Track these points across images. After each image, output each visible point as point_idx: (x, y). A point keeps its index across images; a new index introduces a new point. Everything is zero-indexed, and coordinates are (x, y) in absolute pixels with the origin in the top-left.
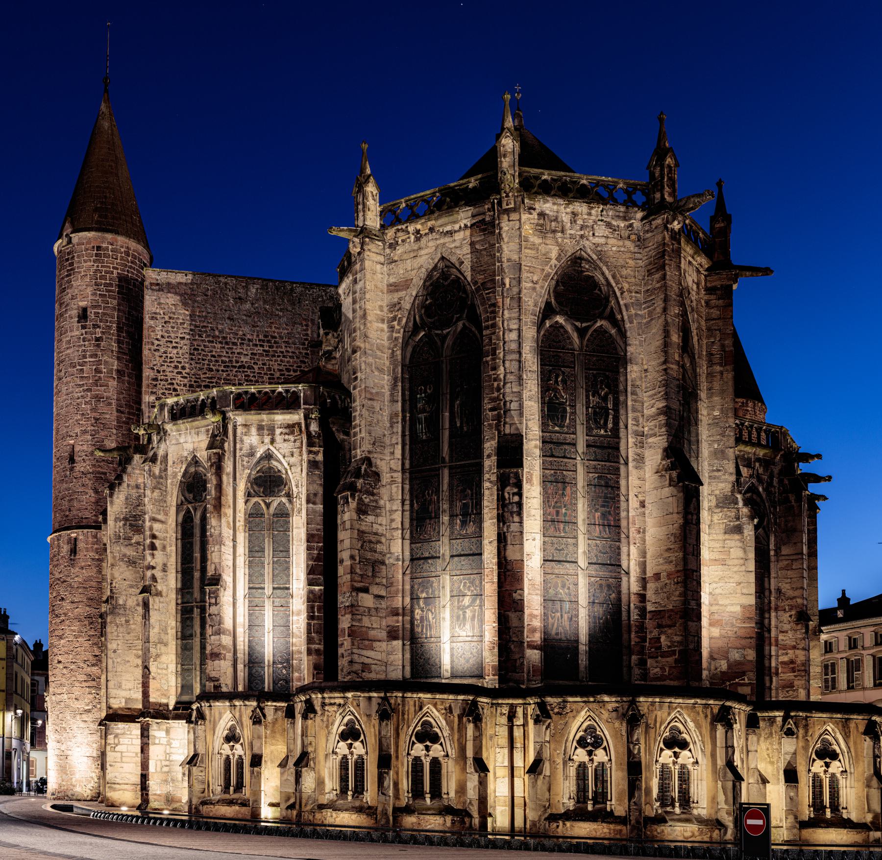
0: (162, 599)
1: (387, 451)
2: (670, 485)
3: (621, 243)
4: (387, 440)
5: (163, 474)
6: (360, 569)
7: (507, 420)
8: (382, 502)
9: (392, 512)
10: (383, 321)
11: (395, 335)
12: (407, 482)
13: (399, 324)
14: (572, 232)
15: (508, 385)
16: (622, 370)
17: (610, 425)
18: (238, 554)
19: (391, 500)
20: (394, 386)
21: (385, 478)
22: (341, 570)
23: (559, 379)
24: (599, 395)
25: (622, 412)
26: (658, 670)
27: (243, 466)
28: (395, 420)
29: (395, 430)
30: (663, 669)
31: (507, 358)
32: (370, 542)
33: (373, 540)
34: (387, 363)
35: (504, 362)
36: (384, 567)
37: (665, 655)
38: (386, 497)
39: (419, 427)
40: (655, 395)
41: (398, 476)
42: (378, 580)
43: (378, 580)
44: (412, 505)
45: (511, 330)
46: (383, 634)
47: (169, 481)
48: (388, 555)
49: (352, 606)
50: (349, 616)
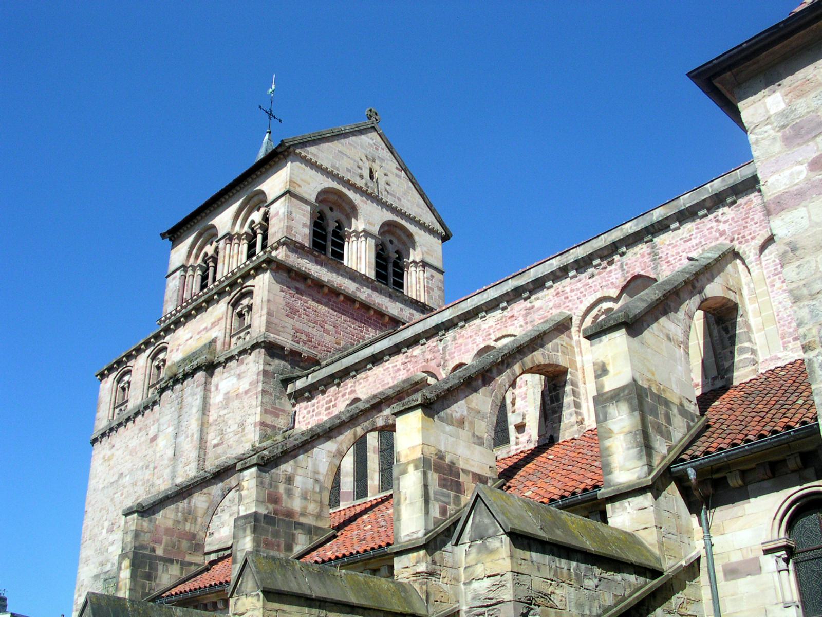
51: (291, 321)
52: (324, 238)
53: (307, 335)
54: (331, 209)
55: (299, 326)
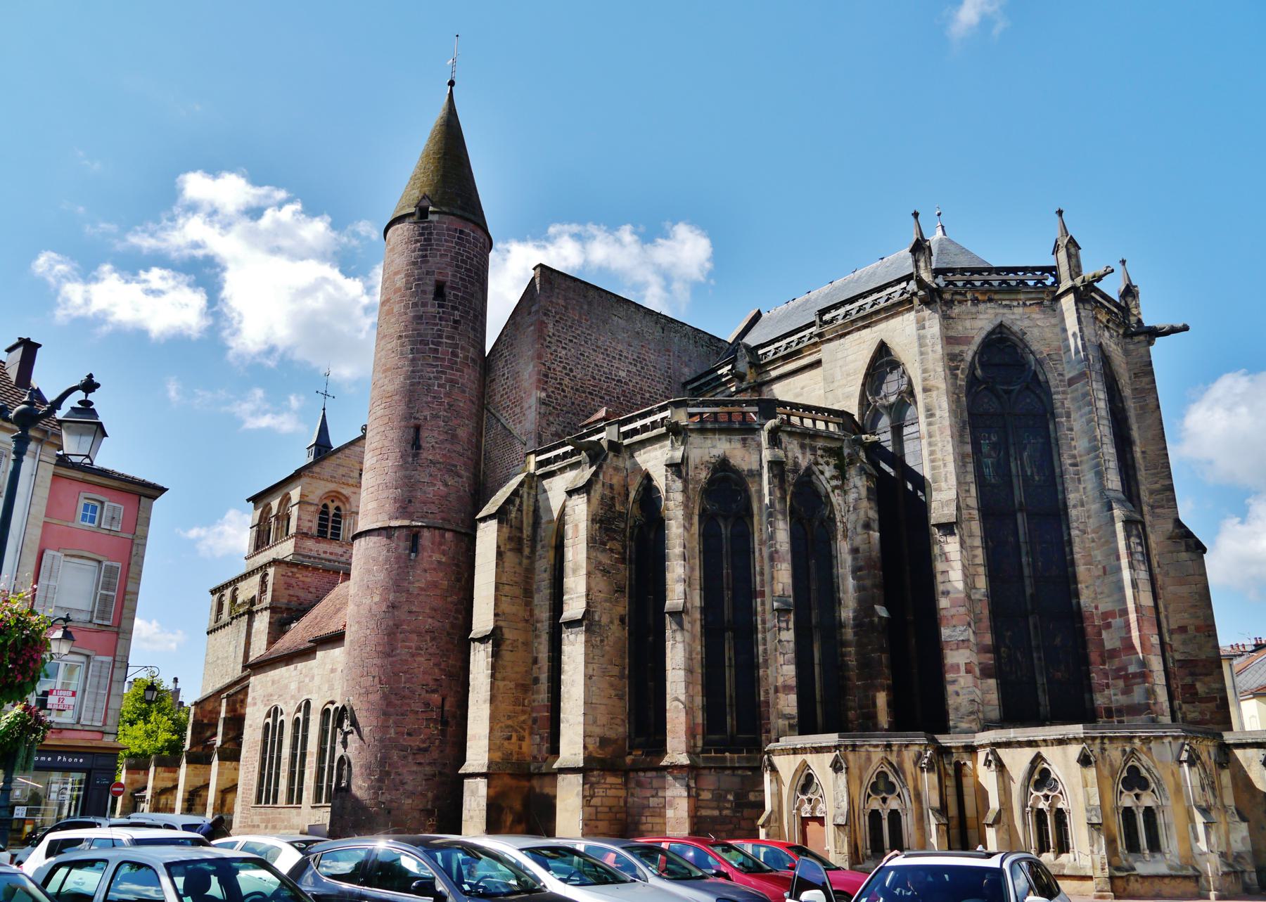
16: (1128, 449)
25: (1133, 483)
35: (1098, 424)
40: (1158, 473)
48: (974, 591)
51: (288, 592)
52: (327, 520)
53: (297, 596)
54: (333, 501)
55: (291, 592)
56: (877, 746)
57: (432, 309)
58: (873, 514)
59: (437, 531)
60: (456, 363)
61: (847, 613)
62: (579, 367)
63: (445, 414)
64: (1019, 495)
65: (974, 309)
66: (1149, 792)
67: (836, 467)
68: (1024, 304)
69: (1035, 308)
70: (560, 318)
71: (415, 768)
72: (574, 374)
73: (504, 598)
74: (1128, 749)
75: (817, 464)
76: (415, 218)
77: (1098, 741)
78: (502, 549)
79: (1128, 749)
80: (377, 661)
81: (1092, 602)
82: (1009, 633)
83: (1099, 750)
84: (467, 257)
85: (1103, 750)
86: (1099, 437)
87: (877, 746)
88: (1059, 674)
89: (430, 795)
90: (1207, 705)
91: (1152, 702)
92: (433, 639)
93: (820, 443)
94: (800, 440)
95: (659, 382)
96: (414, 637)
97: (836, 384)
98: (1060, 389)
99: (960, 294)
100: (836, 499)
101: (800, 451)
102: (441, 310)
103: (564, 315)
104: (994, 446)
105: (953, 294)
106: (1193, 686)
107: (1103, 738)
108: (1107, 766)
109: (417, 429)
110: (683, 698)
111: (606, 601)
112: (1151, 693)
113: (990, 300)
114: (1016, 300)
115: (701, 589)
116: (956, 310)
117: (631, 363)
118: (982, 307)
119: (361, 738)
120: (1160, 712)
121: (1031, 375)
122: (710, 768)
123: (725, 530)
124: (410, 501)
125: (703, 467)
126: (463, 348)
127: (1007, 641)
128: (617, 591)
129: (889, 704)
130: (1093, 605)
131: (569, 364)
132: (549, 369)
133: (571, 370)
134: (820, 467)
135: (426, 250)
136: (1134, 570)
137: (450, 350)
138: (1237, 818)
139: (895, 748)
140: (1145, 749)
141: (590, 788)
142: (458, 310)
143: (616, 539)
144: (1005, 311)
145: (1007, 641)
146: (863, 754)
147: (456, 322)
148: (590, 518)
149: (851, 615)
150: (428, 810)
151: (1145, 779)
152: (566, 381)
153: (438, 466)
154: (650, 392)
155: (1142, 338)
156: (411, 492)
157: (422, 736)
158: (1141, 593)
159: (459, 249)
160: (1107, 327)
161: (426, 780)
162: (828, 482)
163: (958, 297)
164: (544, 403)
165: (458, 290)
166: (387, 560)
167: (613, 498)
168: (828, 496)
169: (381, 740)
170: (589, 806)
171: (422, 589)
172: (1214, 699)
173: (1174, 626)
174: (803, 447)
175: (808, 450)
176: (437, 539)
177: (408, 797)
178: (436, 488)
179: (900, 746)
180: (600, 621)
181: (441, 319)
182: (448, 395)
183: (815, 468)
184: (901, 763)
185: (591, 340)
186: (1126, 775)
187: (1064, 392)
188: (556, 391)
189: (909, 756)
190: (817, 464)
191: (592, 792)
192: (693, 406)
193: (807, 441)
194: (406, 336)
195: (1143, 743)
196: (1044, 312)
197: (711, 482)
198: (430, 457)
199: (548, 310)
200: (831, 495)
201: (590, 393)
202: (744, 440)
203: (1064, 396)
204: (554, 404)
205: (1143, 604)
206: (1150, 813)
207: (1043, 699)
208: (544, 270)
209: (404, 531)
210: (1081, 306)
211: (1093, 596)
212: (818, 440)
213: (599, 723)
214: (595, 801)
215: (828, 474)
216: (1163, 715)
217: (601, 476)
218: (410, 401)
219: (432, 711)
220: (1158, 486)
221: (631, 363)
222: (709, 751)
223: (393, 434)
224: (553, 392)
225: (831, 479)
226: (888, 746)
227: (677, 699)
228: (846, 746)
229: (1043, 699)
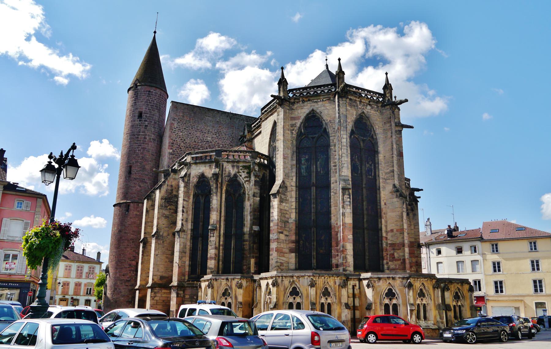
0: (185, 233)
1: (290, 178)
2: (396, 198)
3: (375, 112)
4: (290, 175)
5: (188, 182)
6: (281, 224)
7: (343, 170)
8: (288, 198)
9: (292, 202)
10: (289, 130)
11: (293, 136)
12: (298, 191)
13: (295, 132)
14: (360, 107)
15: (343, 158)
16: (376, 156)
17: (373, 175)
18: (222, 216)
19: (291, 197)
20: (293, 154)
21: (289, 189)
22: (271, 225)
23: (356, 157)
24: (369, 164)
25: (377, 170)
26: (394, 266)
27: (225, 180)
28: (293, 167)
29: (293, 171)
30: (396, 265)
31: (342, 148)
32: (284, 213)
33: (285, 213)
34: (290, 146)
36: (288, 224)
37: (396, 260)
38: (289, 196)
39: (302, 171)
40: (389, 165)
41: (294, 188)
42: (286, 229)
43: (286, 229)
44: (299, 199)
45: (344, 138)
46: (287, 251)
47: (191, 185)
48: (290, 219)
49: (277, 239)
50: (276, 243)
56: (223, 279)
57: (137, 122)
58: (257, 191)
59: (136, 204)
60: (146, 141)
61: (246, 229)
62: (188, 138)
63: (141, 161)
64: (314, 180)
65: (302, 105)
66: (298, 297)
67: (247, 173)
68: (323, 100)
69: (327, 102)
70: (180, 121)
71: (125, 287)
72: (186, 141)
73: (148, 227)
74: (291, 281)
75: (239, 172)
76: (133, 89)
77: (281, 277)
78: (148, 209)
79: (291, 281)
80: (115, 250)
81: (335, 222)
82: (304, 235)
83: (281, 281)
84: (152, 101)
85: (282, 281)
86: (341, 154)
87: (223, 279)
88: (322, 251)
89: (130, 296)
90: (398, 262)
91: (344, 262)
92: (133, 242)
93: (241, 164)
94: (232, 164)
95: (227, 140)
96: (126, 241)
97: (264, 138)
98: (333, 135)
99: (297, 99)
100: (246, 186)
101: (232, 168)
102: (140, 122)
103: (182, 119)
104: (307, 160)
105: (294, 100)
106: (393, 254)
107: (282, 276)
108: (283, 287)
109: (130, 167)
110: (178, 262)
111: (166, 227)
112: (345, 258)
113: (309, 100)
114: (319, 99)
115: (192, 222)
116: (296, 106)
117: (214, 134)
118: (306, 103)
119: (110, 277)
120: (347, 266)
121: (323, 130)
122: (189, 287)
123: (202, 201)
124: (127, 193)
125: (195, 177)
126: (149, 135)
127: (303, 238)
128: (171, 224)
129: (256, 263)
130: (336, 223)
131: (183, 138)
132: (174, 141)
133: (184, 140)
134: (240, 174)
135: (136, 100)
136: (344, 209)
137: (143, 137)
138: (345, 308)
139: (230, 280)
140: (297, 280)
141: (154, 294)
142: (147, 121)
143: (173, 205)
144: (315, 104)
145: (303, 238)
146: (219, 282)
147: (146, 126)
148: (160, 198)
149: (248, 230)
150: (129, 302)
151: (329, 293)
152: (182, 144)
153: (137, 180)
154: (222, 144)
155: (388, 107)
156: (127, 190)
157: (128, 276)
158: (346, 218)
159: (148, 98)
160: (369, 104)
161: (129, 291)
162: (243, 179)
163: (297, 100)
164: (171, 154)
165: (148, 114)
166: (119, 215)
167: (172, 190)
168: (243, 185)
169: (115, 278)
170: (153, 300)
171: (129, 225)
172: (400, 259)
173: (389, 229)
174: (233, 166)
175: (235, 167)
176: (136, 206)
177: (122, 297)
178: (136, 188)
179: (231, 279)
180: (163, 235)
181: (140, 125)
182: (141, 153)
183: (238, 174)
184: (231, 286)
185: (194, 127)
186: (393, 292)
187: (334, 136)
188: (177, 149)
189: (234, 283)
190: (239, 172)
191: (155, 295)
192: (194, 154)
193: (235, 164)
194: (129, 133)
195: (297, 278)
196: (330, 103)
197: (198, 182)
198: (134, 177)
199: (175, 118)
200: (244, 184)
201: (193, 148)
202: (210, 166)
203: (334, 138)
204: (176, 154)
205: (346, 222)
206: (329, 305)
207: (314, 261)
208: (174, 103)
209: (124, 204)
210: (341, 99)
211: (336, 219)
212: (240, 163)
213: (160, 271)
214: (156, 298)
215: (243, 176)
216: (349, 267)
217: (167, 182)
218: (128, 157)
219: (132, 267)
220: (388, 170)
221: (214, 134)
222: (190, 281)
223: (123, 170)
224: (176, 149)
225: (245, 178)
226: (227, 279)
227: (176, 263)
228: (213, 279)
229: (314, 261)
